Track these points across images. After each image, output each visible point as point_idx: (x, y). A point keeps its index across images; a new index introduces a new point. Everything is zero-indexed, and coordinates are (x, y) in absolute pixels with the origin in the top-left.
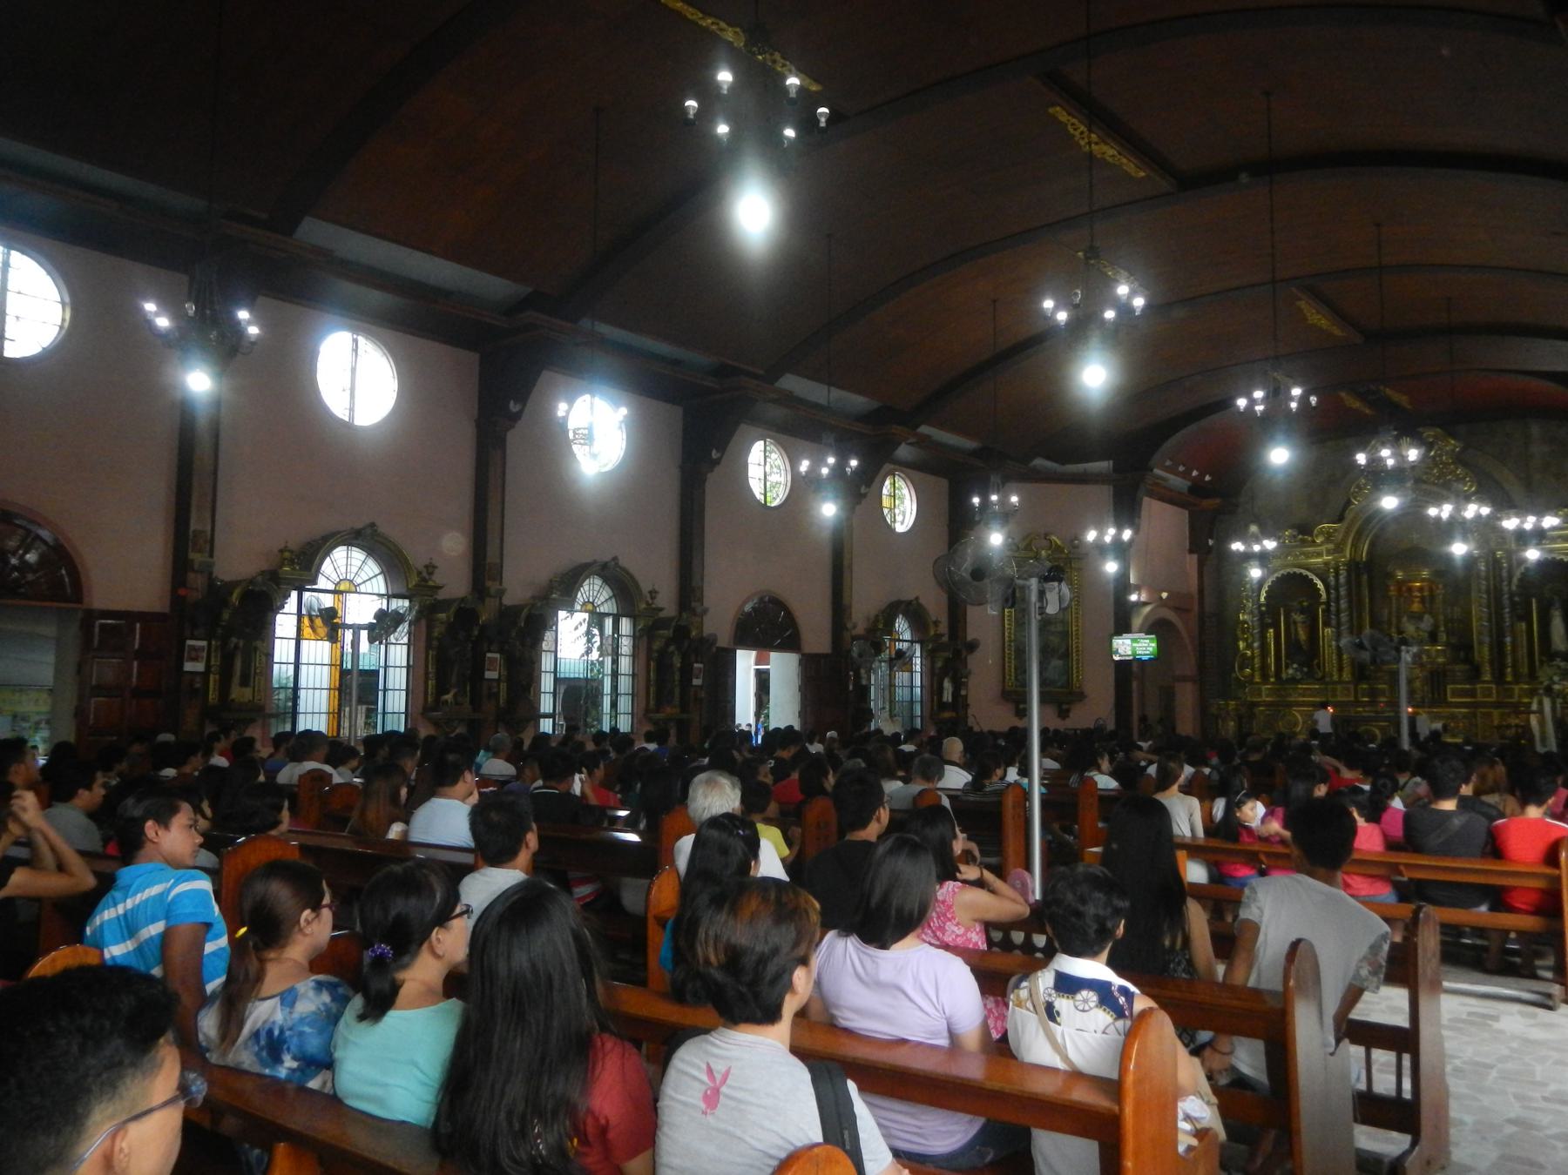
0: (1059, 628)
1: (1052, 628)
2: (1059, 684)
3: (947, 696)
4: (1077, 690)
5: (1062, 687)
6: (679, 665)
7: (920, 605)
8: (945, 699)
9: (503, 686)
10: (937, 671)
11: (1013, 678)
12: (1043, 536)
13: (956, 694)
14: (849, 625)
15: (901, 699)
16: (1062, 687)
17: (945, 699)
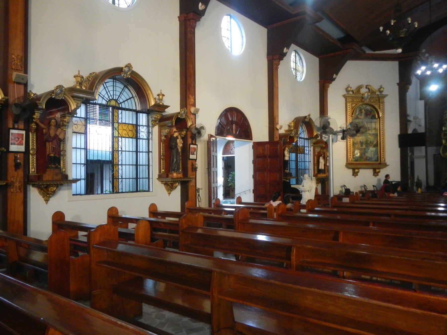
0: (374, 132)
1: (370, 132)
2: (374, 159)
3: (322, 166)
4: (383, 162)
5: (376, 161)
6: (181, 145)
7: (310, 119)
8: (320, 168)
9: (33, 160)
10: (316, 153)
11: (352, 157)
12: (365, 87)
13: (325, 165)
14: (278, 127)
15: (301, 168)
16: (376, 161)
17: (320, 168)
